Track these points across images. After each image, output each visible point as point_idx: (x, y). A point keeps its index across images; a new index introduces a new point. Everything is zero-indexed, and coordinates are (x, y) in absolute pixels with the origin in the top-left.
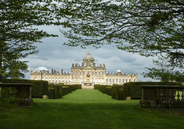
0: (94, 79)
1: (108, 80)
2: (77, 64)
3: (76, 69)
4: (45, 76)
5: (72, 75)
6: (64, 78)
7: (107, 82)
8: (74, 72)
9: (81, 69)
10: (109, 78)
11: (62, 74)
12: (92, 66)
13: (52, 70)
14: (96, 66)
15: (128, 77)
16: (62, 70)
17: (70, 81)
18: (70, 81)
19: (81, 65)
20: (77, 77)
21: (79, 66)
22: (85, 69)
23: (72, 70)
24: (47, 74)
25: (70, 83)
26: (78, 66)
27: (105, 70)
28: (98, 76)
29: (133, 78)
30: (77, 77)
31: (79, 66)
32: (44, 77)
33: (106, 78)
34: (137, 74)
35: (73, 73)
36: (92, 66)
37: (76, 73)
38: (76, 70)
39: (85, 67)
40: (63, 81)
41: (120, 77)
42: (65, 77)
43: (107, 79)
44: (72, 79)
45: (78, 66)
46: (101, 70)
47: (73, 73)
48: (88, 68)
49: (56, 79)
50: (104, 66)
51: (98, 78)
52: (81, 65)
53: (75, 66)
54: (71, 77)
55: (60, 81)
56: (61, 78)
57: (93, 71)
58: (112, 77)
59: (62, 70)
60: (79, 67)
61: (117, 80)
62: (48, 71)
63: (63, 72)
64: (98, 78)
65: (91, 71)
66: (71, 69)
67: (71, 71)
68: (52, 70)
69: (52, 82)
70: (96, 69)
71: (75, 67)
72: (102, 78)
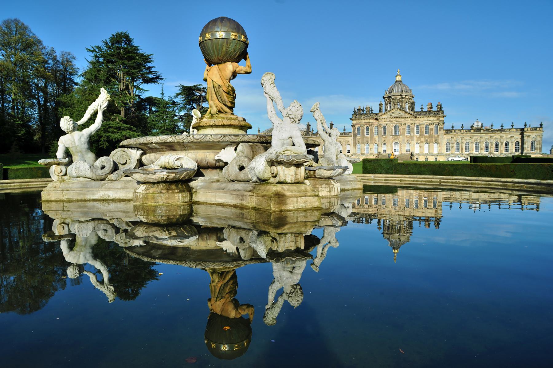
1: (451, 145)
5: (355, 135)
7: (448, 149)
8: (359, 129)
10: (453, 140)
12: (408, 111)
14: (417, 109)
15: (512, 135)
18: (349, 152)
20: (366, 140)
23: (354, 122)
27: (441, 119)
28: (422, 135)
29: (529, 136)
30: (366, 140)
33: (444, 139)
34: (541, 125)
35: (356, 132)
36: (408, 111)
37: (363, 131)
38: (363, 121)
41: (488, 137)
43: (448, 144)
44: (355, 145)
46: (432, 119)
47: (356, 132)
48: (397, 116)
50: (441, 108)
51: (422, 142)
58: (462, 138)
61: (477, 144)
65: (403, 123)
66: (352, 119)
67: (352, 126)
72: (434, 140)
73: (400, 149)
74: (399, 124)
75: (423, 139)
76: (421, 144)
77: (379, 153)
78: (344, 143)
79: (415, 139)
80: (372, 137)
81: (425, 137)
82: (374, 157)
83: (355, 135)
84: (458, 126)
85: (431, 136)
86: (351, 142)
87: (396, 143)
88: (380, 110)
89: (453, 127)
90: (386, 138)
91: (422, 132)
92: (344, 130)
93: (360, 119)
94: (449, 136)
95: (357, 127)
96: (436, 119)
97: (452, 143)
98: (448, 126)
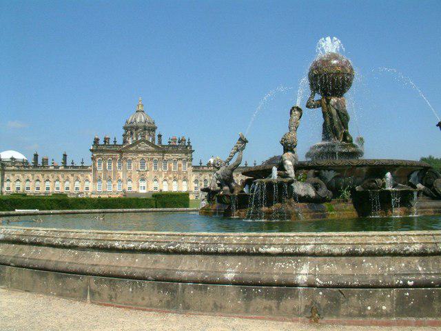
0: (161, 179)
2: (106, 140)
3: (108, 151)
4: (13, 175)
6: (71, 178)
9: (120, 152)
10: (202, 178)
11: (66, 167)
13: (36, 156)
16: (65, 156)
17: (87, 188)
18: (87, 188)
19: (120, 142)
21: (115, 142)
22: (131, 152)
23: (95, 155)
24: (18, 167)
25: (89, 194)
26: (111, 143)
28: (170, 171)
31: (115, 142)
32: (11, 178)
33: (193, 177)
39: (131, 146)
40: (67, 188)
42: (72, 175)
44: (95, 180)
45: (111, 143)
49: (57, 183)
51: (170, 179)
52: (120, 142)
53: (102, 142)
54: (90, 177)
55: (58, 188)
56: (62, 179)
57: (156, 157)
59: (65, 156)
60: (115, 145)
62: (27, 163)
63: (69, 164)
64: (170, 179)
67: (92, 159)
68: (36, 156)
69: (35, 191)
70: (164, 152)
71: (101, 148)
73: (148, 186)
74: (146, 160)
75: (171, 176)
76: (170, 181)
77: (124, 190)
78: (81, 178)
79: (163, 176)
80: (115, 172)
81: (174, 173)
82: (117, 196)
83: (95, 170)
84: (204, 164)
85: (179, 172)
86: (90, 177)
87: (143, 180)
88: (125, 142)
89: (201, 164)
90: (131, 173)
91: (170, 168)
92: (82, 163)
93: (102, 151)
94: (198, 173)
95: (97, 160)
96: (184, 155)
97: (201, 181)
98: (196, 163)
